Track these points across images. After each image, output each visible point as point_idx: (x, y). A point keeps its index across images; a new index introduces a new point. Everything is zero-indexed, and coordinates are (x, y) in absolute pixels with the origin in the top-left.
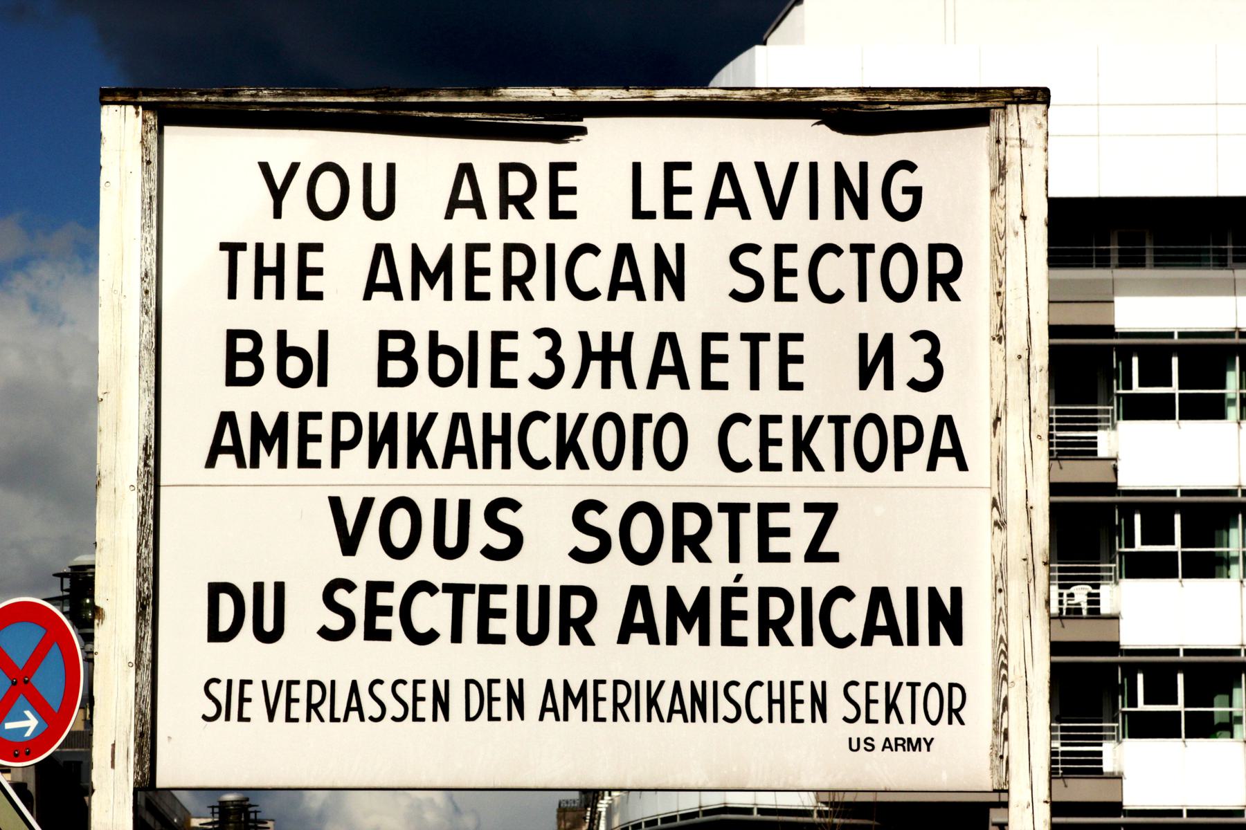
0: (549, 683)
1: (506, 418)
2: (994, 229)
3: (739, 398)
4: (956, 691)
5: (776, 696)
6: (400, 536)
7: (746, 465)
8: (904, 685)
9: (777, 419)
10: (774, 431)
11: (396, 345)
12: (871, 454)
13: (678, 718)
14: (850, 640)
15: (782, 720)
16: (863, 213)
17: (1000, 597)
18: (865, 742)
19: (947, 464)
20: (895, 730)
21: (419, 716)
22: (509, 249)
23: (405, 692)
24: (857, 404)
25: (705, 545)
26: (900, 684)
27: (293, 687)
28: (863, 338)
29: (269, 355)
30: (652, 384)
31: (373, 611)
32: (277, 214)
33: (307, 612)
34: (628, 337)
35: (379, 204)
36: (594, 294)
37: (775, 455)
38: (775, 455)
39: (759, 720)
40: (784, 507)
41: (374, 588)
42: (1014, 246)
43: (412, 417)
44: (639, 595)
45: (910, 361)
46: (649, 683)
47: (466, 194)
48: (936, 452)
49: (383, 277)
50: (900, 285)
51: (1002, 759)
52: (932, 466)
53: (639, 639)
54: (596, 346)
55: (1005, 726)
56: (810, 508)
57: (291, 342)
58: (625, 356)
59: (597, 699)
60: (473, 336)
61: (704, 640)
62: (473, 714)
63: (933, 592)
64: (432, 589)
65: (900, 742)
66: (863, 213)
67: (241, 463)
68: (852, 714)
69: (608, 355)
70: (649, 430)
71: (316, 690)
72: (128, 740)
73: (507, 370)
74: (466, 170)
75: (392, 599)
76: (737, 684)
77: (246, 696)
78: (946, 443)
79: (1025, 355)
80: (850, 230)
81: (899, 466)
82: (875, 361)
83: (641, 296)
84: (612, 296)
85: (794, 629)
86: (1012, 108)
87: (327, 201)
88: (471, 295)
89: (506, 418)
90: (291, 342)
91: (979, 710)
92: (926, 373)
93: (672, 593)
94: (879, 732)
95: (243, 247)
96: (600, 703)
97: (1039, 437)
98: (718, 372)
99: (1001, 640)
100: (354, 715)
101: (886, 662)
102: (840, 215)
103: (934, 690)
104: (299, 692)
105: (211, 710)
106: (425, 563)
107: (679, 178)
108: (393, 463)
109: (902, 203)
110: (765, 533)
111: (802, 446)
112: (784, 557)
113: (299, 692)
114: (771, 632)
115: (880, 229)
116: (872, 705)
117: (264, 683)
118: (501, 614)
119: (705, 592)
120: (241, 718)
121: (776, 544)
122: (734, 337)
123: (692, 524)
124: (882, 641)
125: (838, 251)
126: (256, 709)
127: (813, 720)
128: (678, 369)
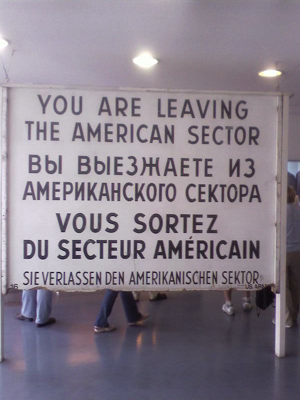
0: (132, 272)
1: (119, 184)
3: (192, 179)
7: (194, 200)
10: (203, 189)
12: (232, 197)
14: (225, 257)
15: (204, 283)
19: (255, 200)
22: (119, 126)
23: (87, 276)
24: (228, 181)
28: (231, 161)
29: (43, 163)
30: (165, 175)
31: (75, 249)
32: (44, 112)
34: (158, 159)
35: (77, 110)
37: (203, 197)
38: (203, 197)
41: (75, 242)
43: (89, 184)
45: (245, 168)
47: (105, 107)
48: (252, 196)
49: (78, 134)
52: (250, 201)
53: (160, 257)
54: (148, 162)
58: (157, 165)
59: (147, 278)
61: (180, 257)
63: (251, 243)
64: (93, 242)
68: (224, 281)
69: (151, 165)
70: (164, 189)
73: (119, 169)
74: (105, 100)
76: (190, 272)
78: (255, 194)
81: (241, 201)
82: (234, 168)
85: (208, 253)
89: (119, 184)
92: (249, 172)
93: (171, 243)
95: (32, 123)
98: (186, 171)
102: (222, 117)
107: (173, 104)
108: (83, 199)
109: (242, 114)
111: (211, 195)
115: (235, 122)
122: (191, 160)
128: (174, 170)
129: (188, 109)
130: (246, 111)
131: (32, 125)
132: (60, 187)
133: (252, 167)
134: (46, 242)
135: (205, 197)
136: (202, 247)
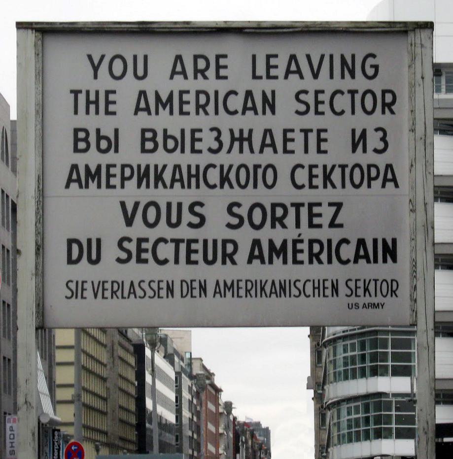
1: (198, 167)
2: (410, 84)
3: (298, 157)
4: (395, 284)
5: (316, 285)
6: (151, 217)
7: (303, 186)
8: (372, 280)
9: (316, 166)
10: (315, 171)
13: (274, 296)
14: (348, 261)
15: (319, 296)
16: (353, 77)
17: (413, 242)
18: (355, 305)
19: (390, 185)
20: (368, 300)
22: (198, 93)
23: (155, 286)
24: (351, 159)
25: (285, 221)
26: (370, 280)
28: (353, 131)
29: (93, 139)
30: (261, 151)
31: (140, 250)
32: (96, 77)
33: (110, 252)
34: (251, 131)
35: (140, 73)
36: (236, 112)
37: (315, 182)
38: (315, 182)
39: (309, 296)
40: (319, 204)
41: (140, 241)
42: (419, 90)
43: (156, 167)
45: (374, 140)
46: (261, 281)
49: (143, 105)
50: (369, 107)
51: (414, 312)
52: (383, 186)
53: (256, 262)
54: (237, 135)
56: (330, 204)
58: (249, 139)
59: (238, 288)
60: (183, 131)
61: (285, 262)
62: (184, 294)
63: (384, 241)
64: (165, 241)
66: (353, 77)
67: (81, 187)
68: (349, 293)
69: (242, 139)
71: (116, 286)
72: (33, 307)
73: (198, 145)
74: (179, 58)
75: (148, 246)
76: (299, 281)
77: (85, 287)
78: (390, 176)
79: (423, 137)
80: (348, 84)
81: (369, 186)
82: (358, 141)
83: (256, 113)
84: (244, 113)
85: (324, 257)
86: (418, 31)
87: (118, 71)
88: (182, 112)
89: (198, 167)
91: (404, 290)
92: (381, 146)
93: (271, 242)
94: (361, 301)
95: (80, 92)
97: (430, 173)
98: (290, 146)
99: (414, 259)
100: (132, 296)
101: (364, 270)
102: (343, 77)
103: (385, 283)
104: (108, 286)
107: (273, 62)
108: (148, 186)
109: (370, 72)
110: (311, 215)
111: (327, 178)
112: (319, 226)
113: (108, 286)
115: (360, 83)
117: (92, 282)
118: (196, 251)
120: (82, 297)
121: (316, 221)
122: (297, 131)
123: (279, 212)
124: (362, 262)
125: (342, 93)
126: (89, 293)
127: (333, 296)
128: (273, 145)
129: (293, 69)
130: (376, 67)
131: (79, 95)
132: (116, 171)
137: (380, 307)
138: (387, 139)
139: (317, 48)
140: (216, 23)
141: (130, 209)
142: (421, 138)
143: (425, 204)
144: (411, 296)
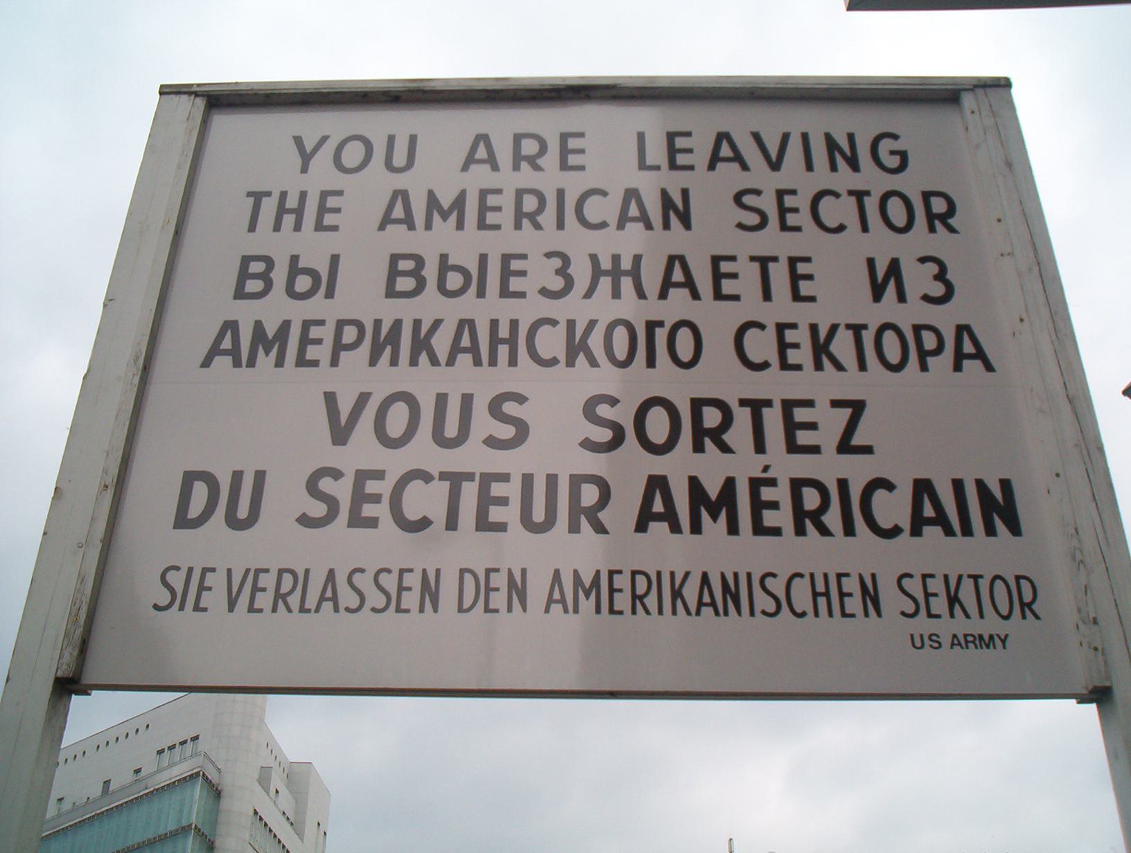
0: (557, 572)
1: (514, 324)
3: (751, 307)
4: (1025, 585)
5: (820, 588)
7: (765, 366)
9: (794, 326)
10: (790, 336)
11: (405, 265)
13: (707, 611)
14: (895, 532)
16: (855, 167)
20: (960, 625)
21: (403, 606)
22: (520, 193)
23: (389, 582)
24: (874, 315)
26: (960, 577)
27: (262, 576)
28: (871, 263)
29: (279, 276)
30: (663, 295)
31: (360, 497)
32: (304, 170)
35: (399, 159)
36: (603, 225)
37: (793, 356)
38: (793, 356)
39: (803, 614)
41: (362, 476)
43: (417, 323)
44: (657, 484)
45: (919, 280)
46: (672, 574)
48: (959, 359)
49: (398, 212)
52: (958, 367)
53: (659, 529)
54: (606, 264)
55: (1092, 615)
56: (836, 404)
57: (301, 265)
58: (635, 273)
59: (612, 590)
60: (483, 259)
61: (733, 529)
62: (466, 605)
63: (980, 484)
64: (426, 477)
65: (970, 638)
66: (855, 167)
67: (237, 363)
68: (910, 608)
70: (661, 335)
71: (288, 581)
73: (515, 284)
75: (383, 488)
76: (774, 575)
78: (968, 348)
79: (1036, 269)
81: (924, 367)
82: (885, 280)
85: (833, 518)
86: (980, 92)
89: (514, 324)
90: (301, 265)
92: (938, 290)
93: (694, 483)
94: (946, 627)
96: (616, 595)
98: (728, 287)
102: (834, 168)
103: (998, 583)
104: (267, 581)
105: (164, 598)
106: (423, 452)
107: (680, 143)
108: (394, 362)
110: (791, 427)
111: (821, 350)
112: (815, 450)
113: (267, 581)
114: (808, 523)
115: (873, 180)
116: (932, 599)
117: (229, 571)
118: (503, 501)
119: (730, 484)
120: (197, 608)
121: (803, 437)
125: (837, 195)
127: (867, 615)
128: (689, 284)
130: (903, 156)
132: (326, 333)
133: (941, 276)
134: (260, 476)
135: (802, 356)
136: (811, 499)
137: (998, 642)
138: (948, 276)
139: (773, 122)
140: (564, 79)
141: (345, 409)
142: (1030, 270)
143: (1070, 401)
144: (1079, 610)
